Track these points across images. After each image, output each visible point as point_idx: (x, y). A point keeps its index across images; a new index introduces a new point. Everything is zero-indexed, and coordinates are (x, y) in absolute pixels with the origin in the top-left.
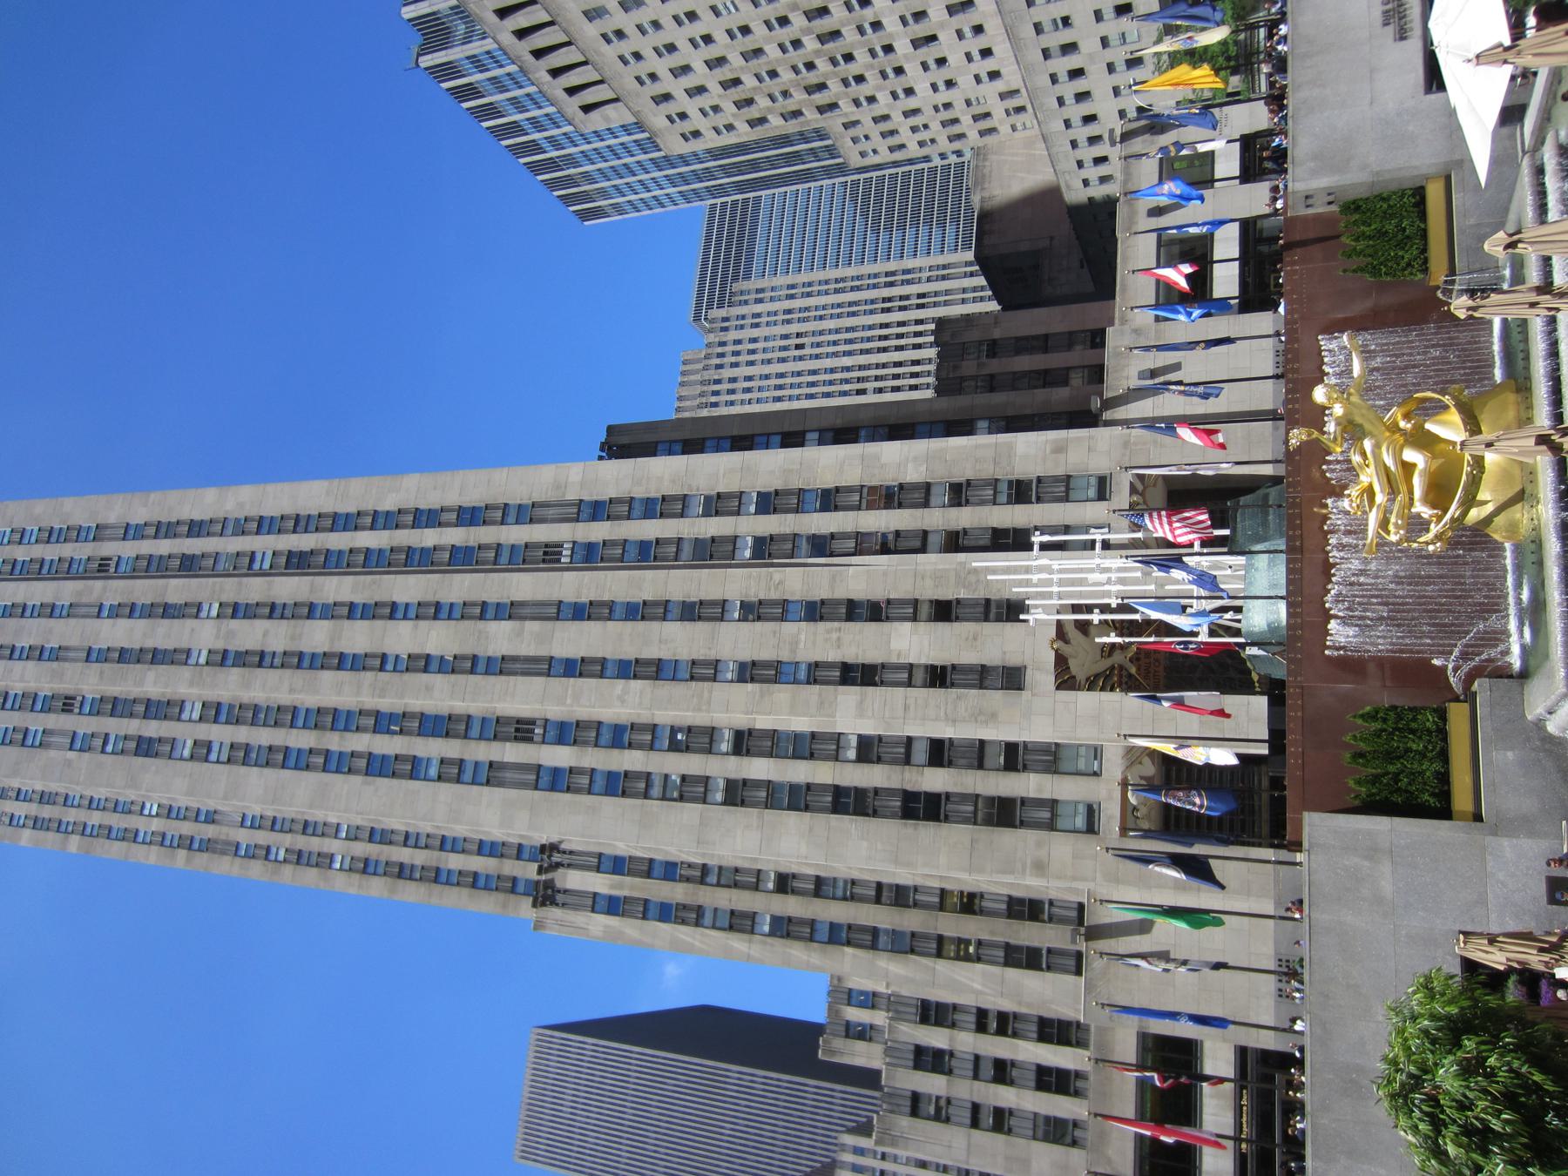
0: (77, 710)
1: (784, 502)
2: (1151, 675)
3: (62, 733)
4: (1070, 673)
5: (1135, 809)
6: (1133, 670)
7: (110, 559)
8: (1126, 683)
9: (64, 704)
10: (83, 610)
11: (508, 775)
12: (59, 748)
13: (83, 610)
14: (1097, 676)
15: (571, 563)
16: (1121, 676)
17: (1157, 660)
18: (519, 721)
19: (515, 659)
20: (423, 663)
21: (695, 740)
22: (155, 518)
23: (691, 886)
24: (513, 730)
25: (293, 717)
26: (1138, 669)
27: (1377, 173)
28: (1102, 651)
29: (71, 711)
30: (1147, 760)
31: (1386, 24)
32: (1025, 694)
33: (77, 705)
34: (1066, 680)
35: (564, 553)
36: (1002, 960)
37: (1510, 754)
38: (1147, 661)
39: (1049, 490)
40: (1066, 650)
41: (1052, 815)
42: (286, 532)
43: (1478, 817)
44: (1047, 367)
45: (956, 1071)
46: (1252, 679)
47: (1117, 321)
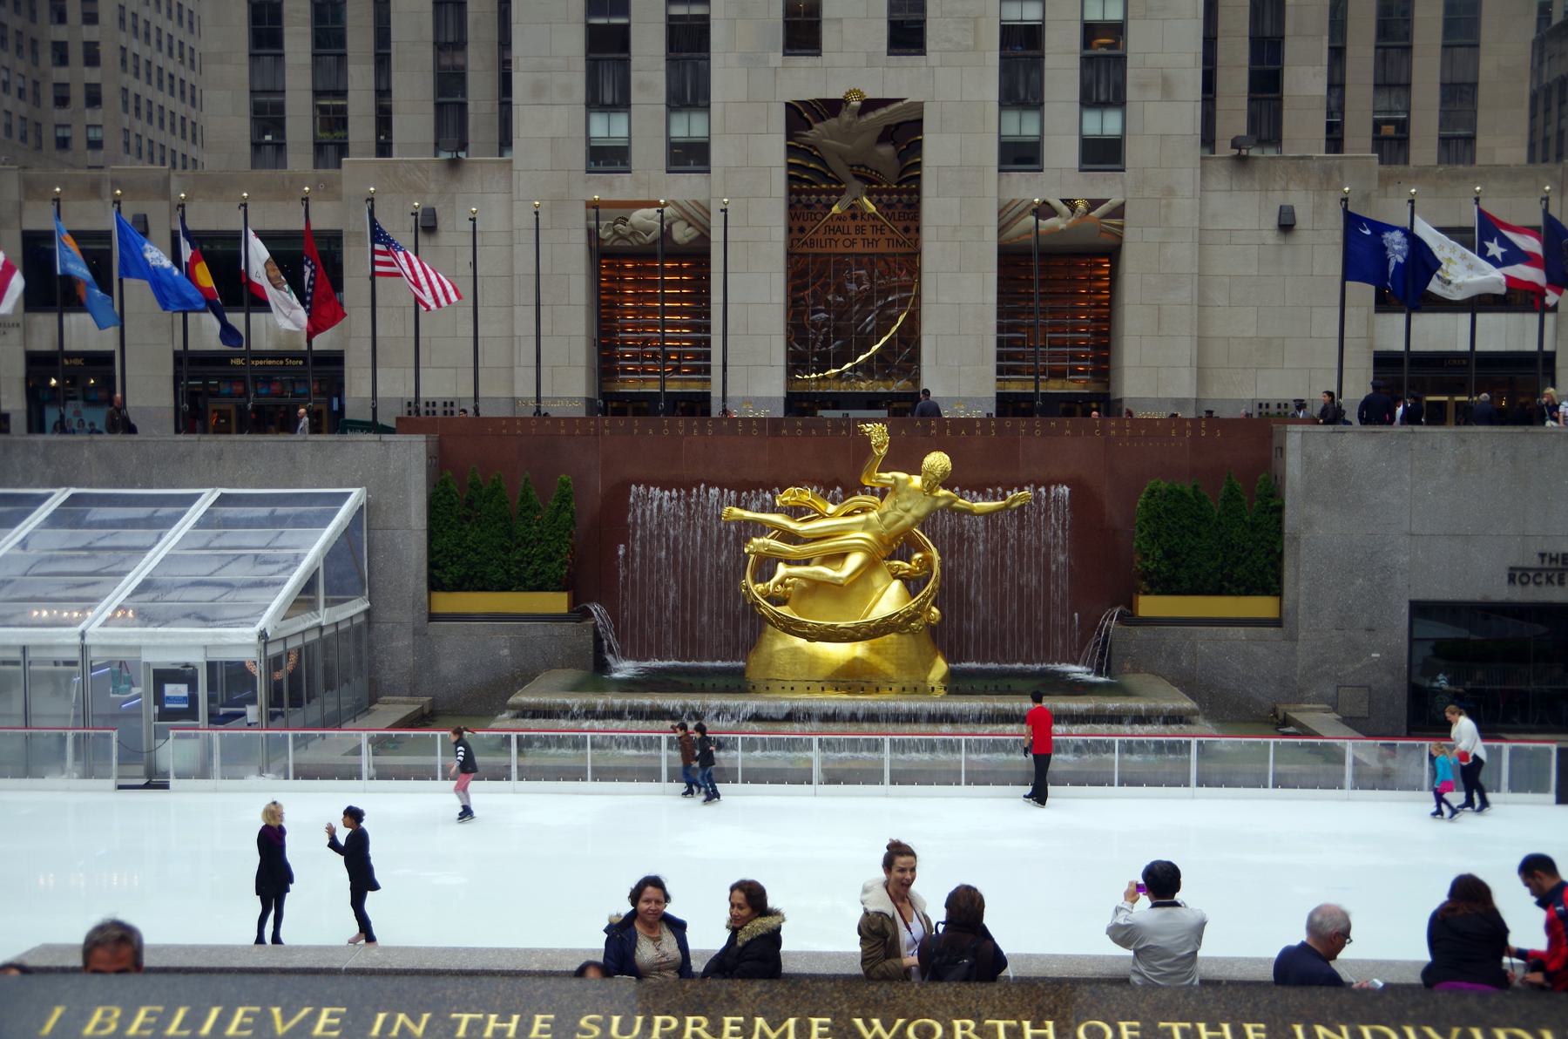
2: (832, 236)
4: (816, 122)
5: (624, 220)
6: (835, 209)
8: (819, 201)
14: (821, 160)
16: (828, 192)
17: (853, 243)
26: (839, 217)
27: (1296, 539)
28: (859, 166)
30: (691, 233)
31: (1542, 555)
32: (777, 57)
34: (800, 116)
36: (442, 39)
37: (506, 652)
38: (852, 230)
39: (1103, 79)
40: (846, 116)
41: (609, 106)
43: (433, 617)
44: (1416, 51)
46: (829, 369)
47: (1384, 168)
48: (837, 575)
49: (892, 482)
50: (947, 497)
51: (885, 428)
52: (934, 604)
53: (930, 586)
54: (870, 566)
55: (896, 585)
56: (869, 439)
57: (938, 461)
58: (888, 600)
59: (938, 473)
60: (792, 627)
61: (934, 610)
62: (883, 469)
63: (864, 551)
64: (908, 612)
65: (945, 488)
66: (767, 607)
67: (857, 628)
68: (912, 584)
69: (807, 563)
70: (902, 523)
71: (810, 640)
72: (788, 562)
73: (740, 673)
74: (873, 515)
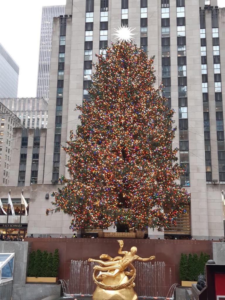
1: (182, 81)
35: (165, 5)
37: (41, 291)
43: (27, 283)
45: (34, 149)
48: (112, 274)
49: (124, 253)
50: (137, 257)
51: (123, 241)
52: (134, 282)
53: (132, 277)
54: (120, 272)
55: (126, 277)
56: (119, 243)
57: (134, 249)
58: (124, 280)
59: (134, 251)
60: (102, 287)
61: (134, 283)
62: (122, 250)
63: (119, 269)
64: (127, 283)
65: (136, 255)
66: (96, 282)
67: (115, 287)
68: (129, 277)
69: (107, 271)
70: (127, 263)
71: (105, 290)
72: (103, 271)
73: (92, 297)
74: (121, 261)
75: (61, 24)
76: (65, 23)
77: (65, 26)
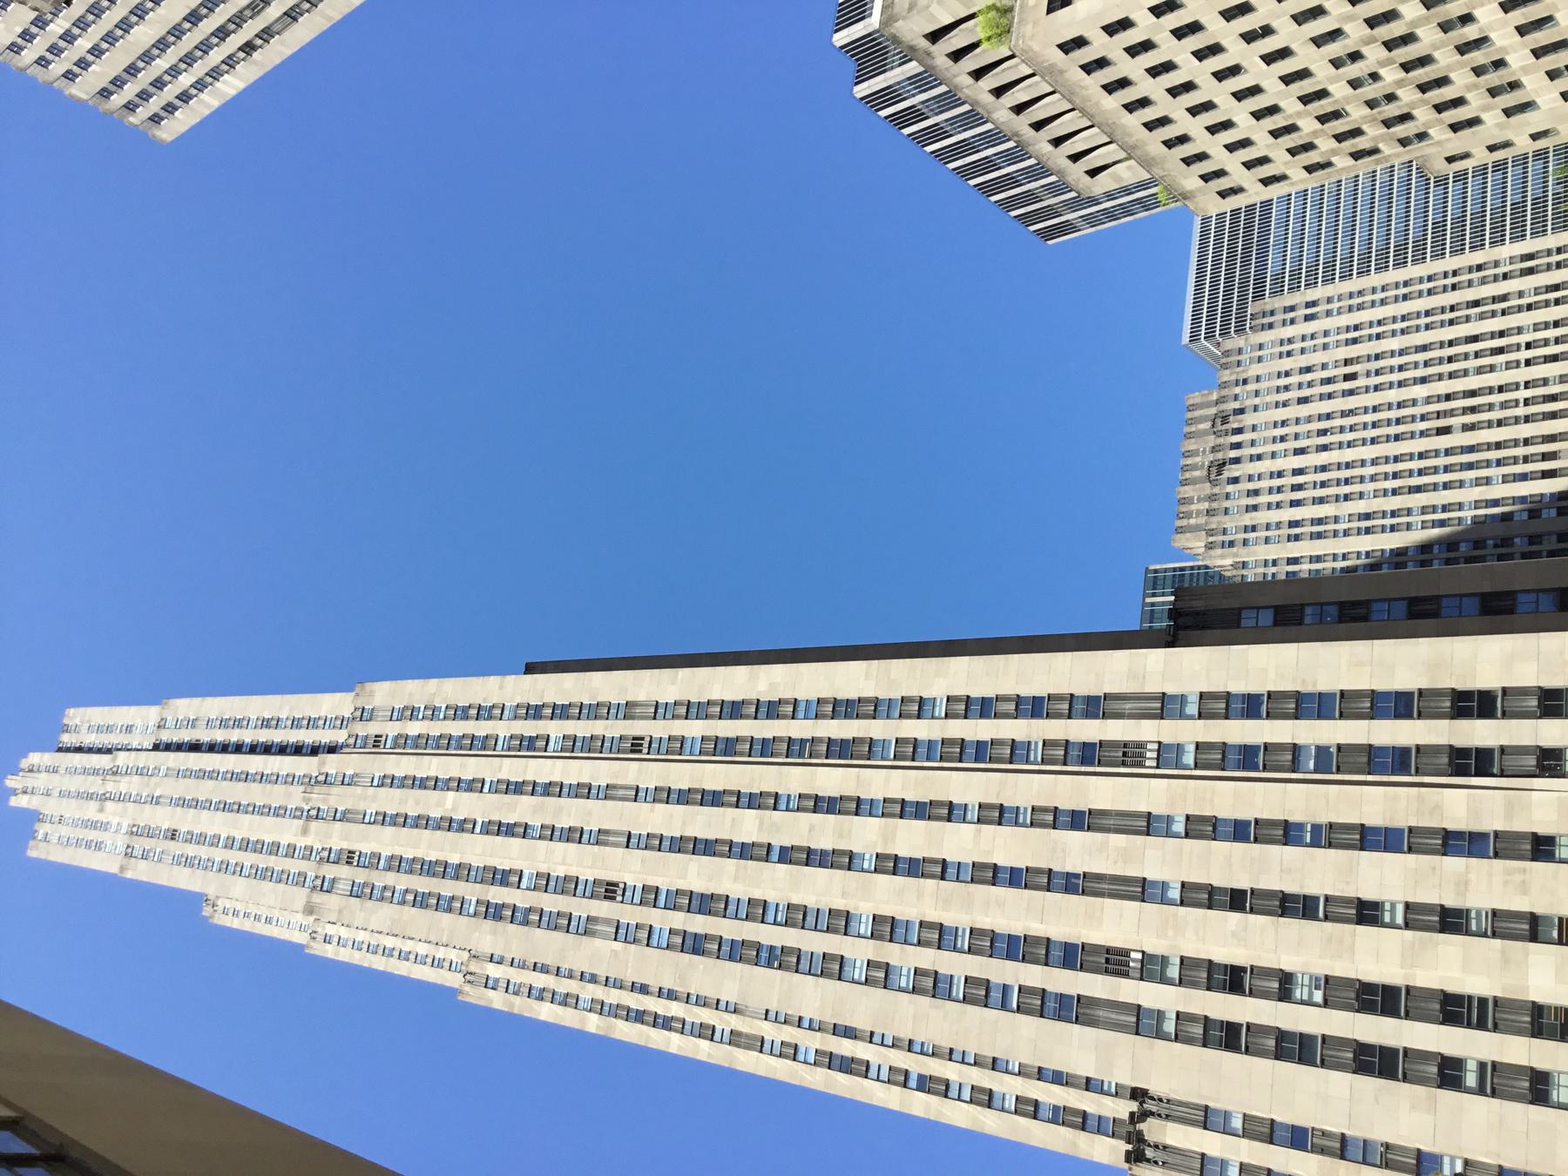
0: (619, 898)
1: (1432, 704)
3: (607, 921)
7: (643, 739)
9: (606, 891)
10: (621, 792)
11: (1102, 1013)
12: (605, 937)
13: (621, 792)
15: (1158, 767)
18: (1108, 950)
19: (1099, 877)
20: (989, 874)
21: (1337, 994)
22: (684, 697)
23: (1327, 1159)
24: (1104, 961)
25: (846, 922)
29: (613, 899)
33: (620, 892)
35: (1149, 755)
42: (824, 717)
75: (1156, 1162)
76: (1156, 1147)
77: (1165, 1147)
